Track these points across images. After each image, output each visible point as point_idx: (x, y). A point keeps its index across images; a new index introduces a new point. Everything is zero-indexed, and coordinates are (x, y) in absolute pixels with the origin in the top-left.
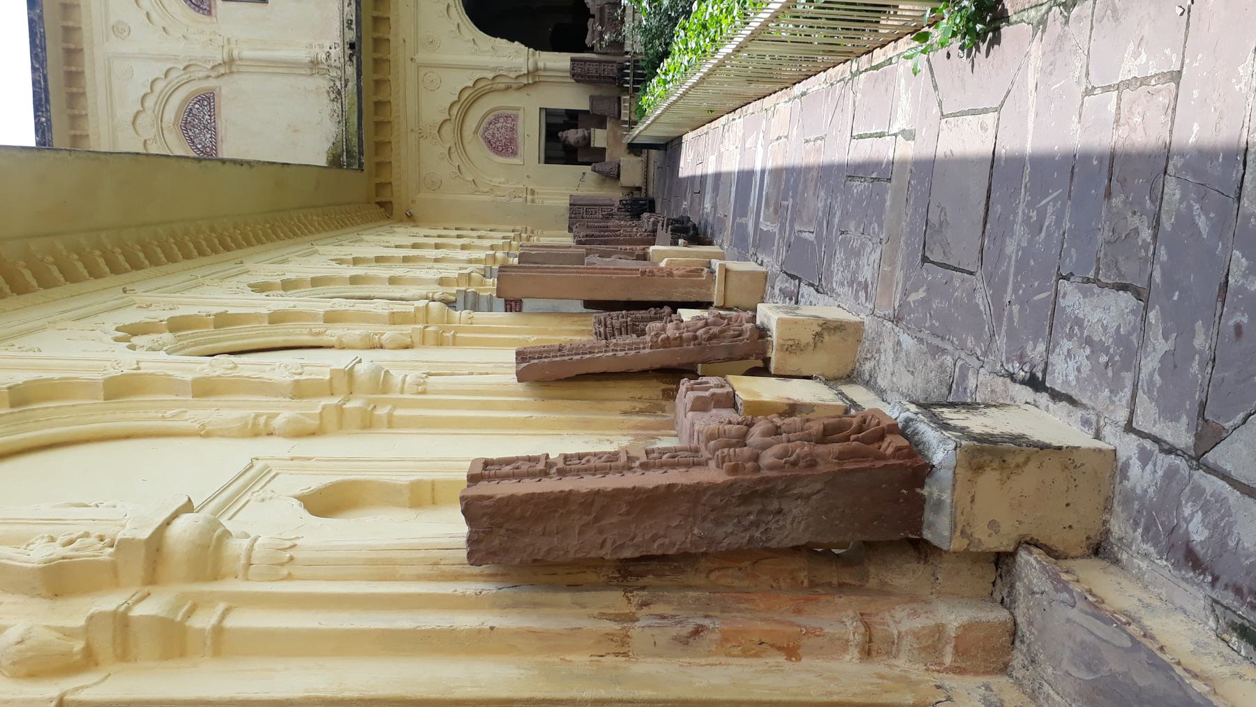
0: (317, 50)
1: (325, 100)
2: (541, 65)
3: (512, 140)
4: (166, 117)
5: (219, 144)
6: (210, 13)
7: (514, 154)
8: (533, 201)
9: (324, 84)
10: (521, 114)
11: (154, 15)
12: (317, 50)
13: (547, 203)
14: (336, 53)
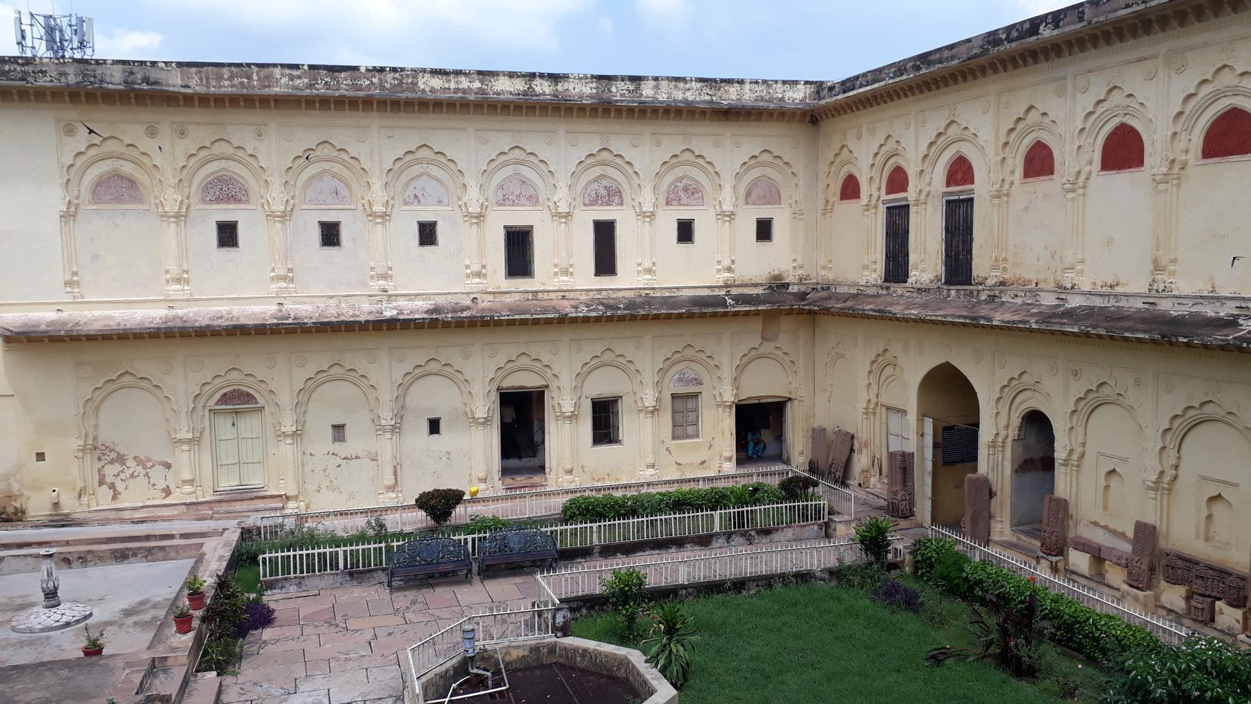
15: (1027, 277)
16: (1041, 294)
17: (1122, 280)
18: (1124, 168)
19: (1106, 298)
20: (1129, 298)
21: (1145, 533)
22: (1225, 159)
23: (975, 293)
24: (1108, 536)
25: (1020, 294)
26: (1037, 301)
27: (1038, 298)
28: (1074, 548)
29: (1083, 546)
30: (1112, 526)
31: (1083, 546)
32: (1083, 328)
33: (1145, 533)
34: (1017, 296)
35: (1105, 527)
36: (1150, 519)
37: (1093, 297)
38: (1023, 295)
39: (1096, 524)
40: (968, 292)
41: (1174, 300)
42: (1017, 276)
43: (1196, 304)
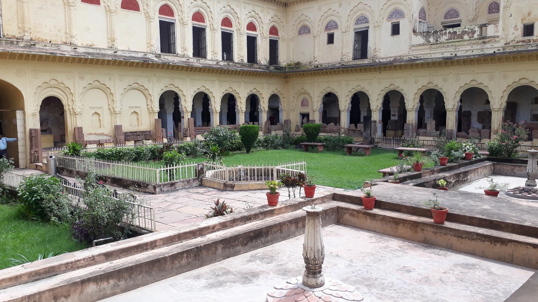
0: (318, 58)
1: (309, 60)
2: (315, 112)
3: (304, 106)
4: (305, 22)
5: (301, 35)
6: (325, 30)
7: (301, 106)
8: (291, 111)
9: (312, 60)
10: (308, 108)
11: (323, 17)
12: (318, 58)
13: (291, 115)
14: (317, 63)
15: (44, 38)
16: (61, 46)
17: (95, 44)
18: (92, 4)
19: (95, 50)
20: (105, 50)
21: (118, 128)
22: (129, 11)
23: (15, 43)
24: (96, 136)
25: (48, 45)
26: (59, 48)
27: (60, 47)
28: (90, 144)
29: (91, 142)
30: (98, 132)
31: (91, 142)
32: (114, 58)
33: (118, 128)
34: (46, 46)
35: (95, 134)
36: (118, 124)
37: (89, 49)
38: (50, 45)
39: (90, 134)
40: (9, 42)
41: (122, 52)
42: (38, 37)
43: (130, 53)
